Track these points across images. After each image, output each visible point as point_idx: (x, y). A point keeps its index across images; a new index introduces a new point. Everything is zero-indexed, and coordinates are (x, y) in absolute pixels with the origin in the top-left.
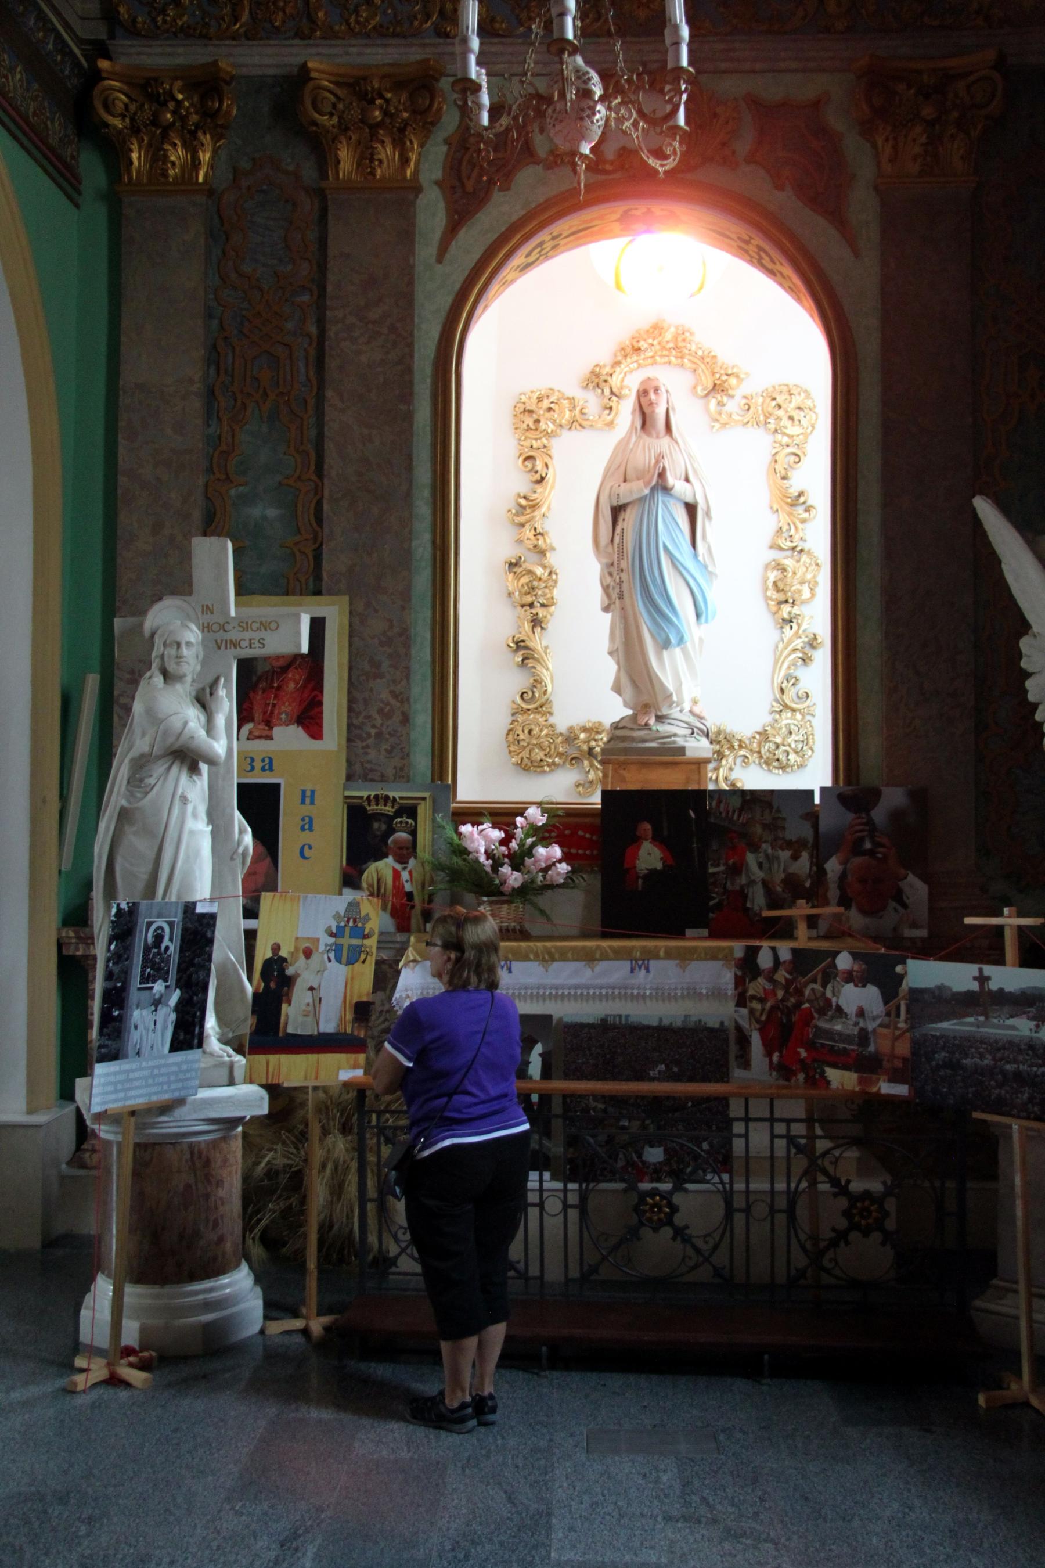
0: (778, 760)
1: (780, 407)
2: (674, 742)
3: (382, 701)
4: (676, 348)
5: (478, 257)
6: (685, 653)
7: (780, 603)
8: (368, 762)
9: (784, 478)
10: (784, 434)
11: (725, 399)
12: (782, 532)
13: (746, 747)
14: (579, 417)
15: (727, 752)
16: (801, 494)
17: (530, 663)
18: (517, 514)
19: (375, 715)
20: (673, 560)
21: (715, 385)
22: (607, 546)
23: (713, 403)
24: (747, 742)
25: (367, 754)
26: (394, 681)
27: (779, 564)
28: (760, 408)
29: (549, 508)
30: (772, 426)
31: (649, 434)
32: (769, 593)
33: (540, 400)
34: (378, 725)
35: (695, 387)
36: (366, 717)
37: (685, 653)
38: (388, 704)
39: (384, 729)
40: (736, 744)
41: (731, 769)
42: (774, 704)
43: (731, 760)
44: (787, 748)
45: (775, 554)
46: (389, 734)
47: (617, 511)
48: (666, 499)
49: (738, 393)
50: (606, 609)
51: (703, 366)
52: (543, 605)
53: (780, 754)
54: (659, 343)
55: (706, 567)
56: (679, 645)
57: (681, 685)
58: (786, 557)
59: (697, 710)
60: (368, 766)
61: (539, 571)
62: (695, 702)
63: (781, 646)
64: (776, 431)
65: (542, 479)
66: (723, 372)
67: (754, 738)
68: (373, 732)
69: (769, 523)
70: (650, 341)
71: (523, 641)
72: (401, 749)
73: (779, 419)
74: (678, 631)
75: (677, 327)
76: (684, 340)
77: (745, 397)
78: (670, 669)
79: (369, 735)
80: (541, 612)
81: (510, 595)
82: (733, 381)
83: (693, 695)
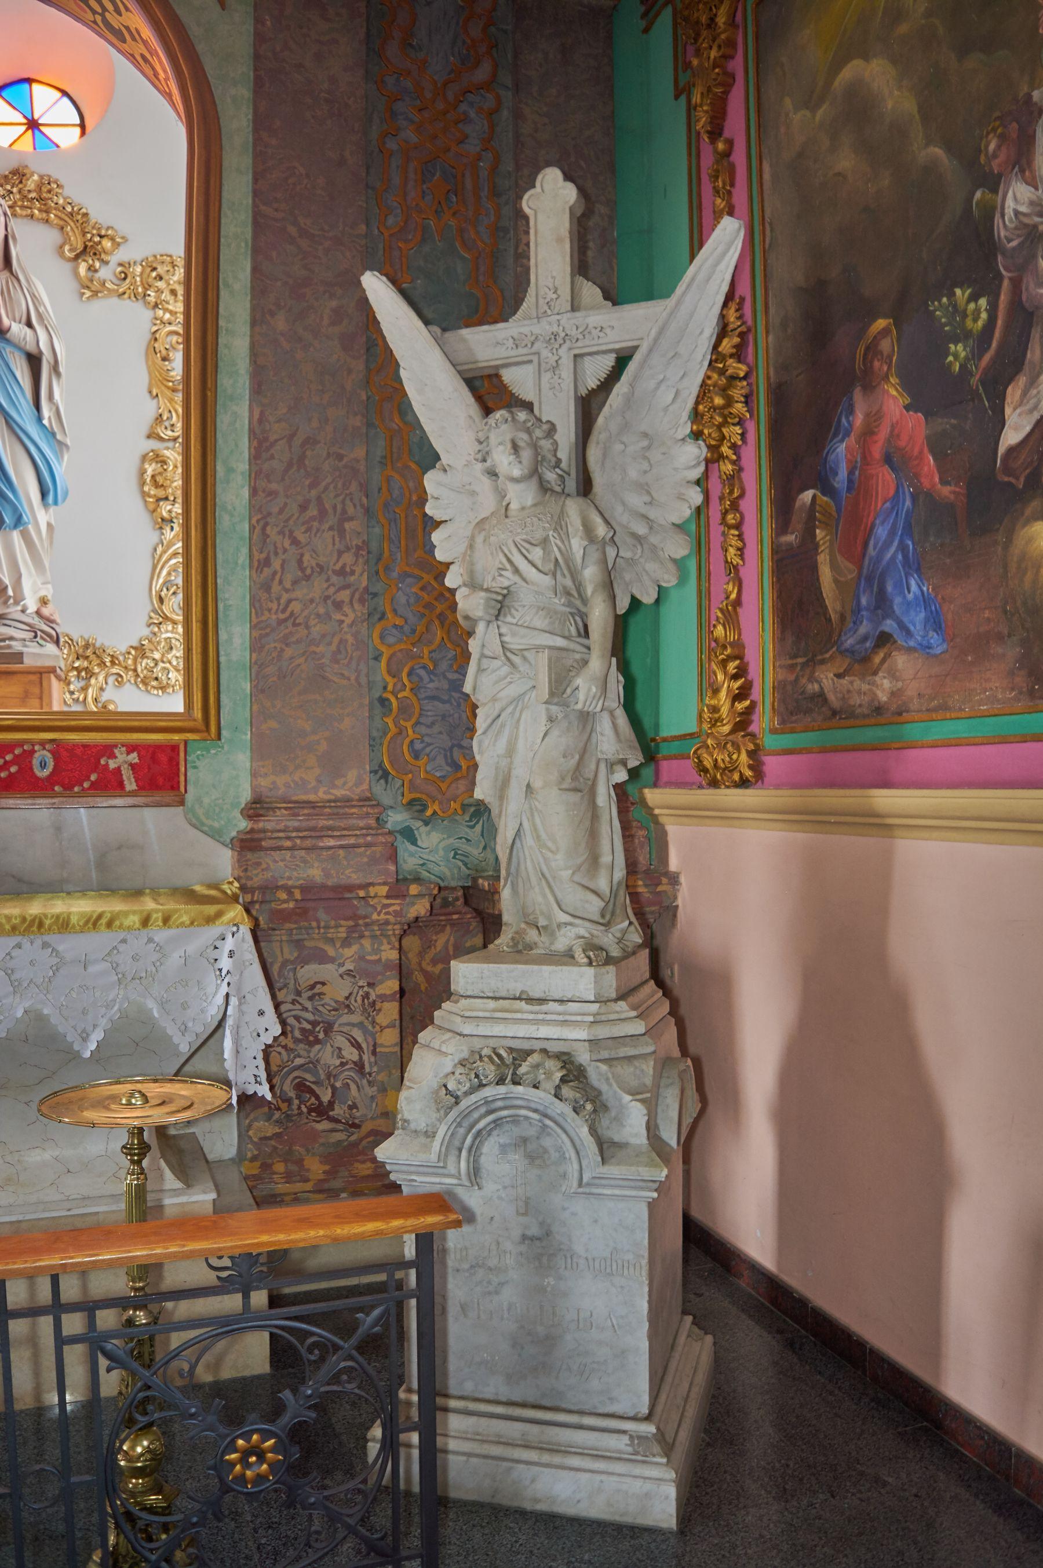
0: (156, 679)
1: (161, 278)
2: (9, 647)
4: (40, 199)
6: (26, 536)
9: (164, 359)
10: (166, 310)
11: (97, 264)
12: (162, 421)
13: (120, 664)
15: (96, 670)
21: (86, 247)
24: (121, 658)
27: (157, 456)
28: (138, 279)
30: (152, 299)
32: (146, 489)
35: (61, 247)
37: (26, 536)
40: (108, 660)
41: (102, 689)
42: (152, 615)
43: (101, 678)
44: (168, 665)
45: (154, 444)
49: (114, 259)
51: (72, 224)
53: (158, 672)
54: (20, 192)
55: (54, 434)
56: (15, 527)
57: (20, 576)
58: (167, 448)
59: (45, 611)
62: (44, 601)
63: (160, 549)
64: (156, 306)
66: (95, 232)
67: (129, 653)
70: (8, 187)
73: (159, 291)
74: (15, 509)
75: (41, 177)
76: (49, 191)
77: (121, 265)
82: (107, 244)
83: (42, 593)
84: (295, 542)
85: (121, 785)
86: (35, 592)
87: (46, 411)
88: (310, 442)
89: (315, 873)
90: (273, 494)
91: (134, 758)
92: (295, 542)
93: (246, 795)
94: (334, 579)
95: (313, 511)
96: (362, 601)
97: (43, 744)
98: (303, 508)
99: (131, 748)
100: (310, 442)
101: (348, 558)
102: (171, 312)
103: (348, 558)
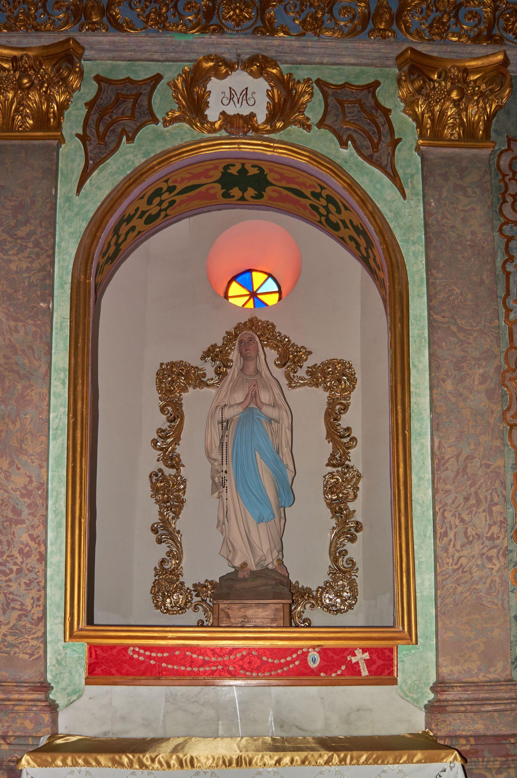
3: (22, 543)
5: (107, 192)
8: (11, 593)
19: (16, 553)
25: (9, 586)
26: (32, 526)
34: (19, 563)
36: (8, 556)
38: (27, 545)
39: (24, 566)
46: (28, 570)
60: (11, 596)
68: (15, 568)
72: (38, 583)
79: (11, 571)
84: (462, 521)
85: (359, 673)
88: (470, 458)
89: (479, 727)
90: (448, 492)
91: (367, 656)
92: (462, 521)
93: (433, 679)
94: (487, 543)
95: (472, 501)
96: (505, 555)
97: (314, 647)
98: (467, 499)
99: (364, 650)
100: (470, 458)
101: (495, 529)
103: (495, 529)
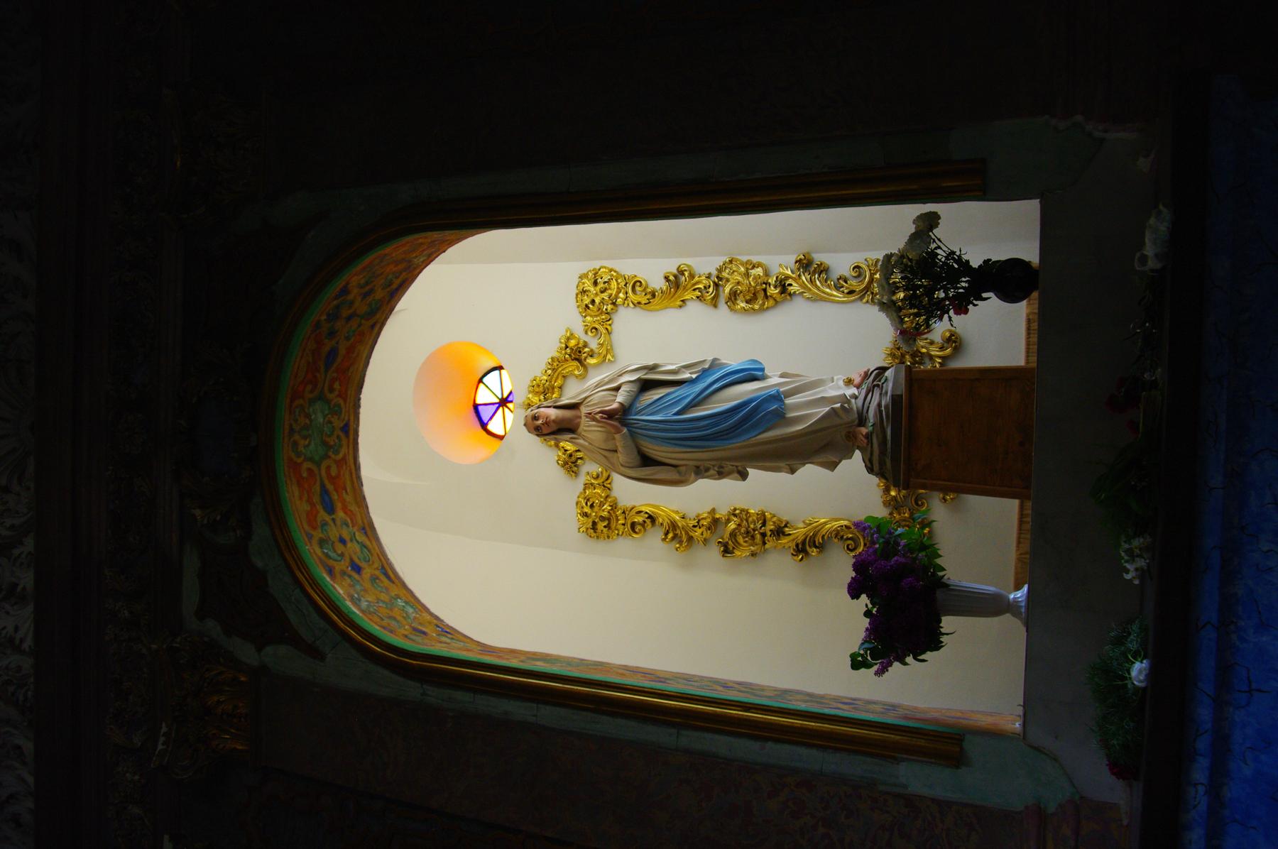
1: (593, 302)
2: (886, 407)
7: (766, 297)
9: (654, 296)
10: (617, 297)
14: (600, 481)
16: (667, 278)
17: (819, 539)
18: (681, 542)
20: (695, 403)
22: (679, 473)
23: (591, 361)
29: (677, 512)
30: (610, 307)
31: (578, 425)
32: (757, 307)
33: (586, 515)
41: (932, 343)
45: (722, 300)
47: (646, 461)
48: (634, 410)
49: (584, 338)
50: (744, 476)
52: (764, 524)
55: (704, 371)
57: (823, 398)
59: (857, 380)
61: (732, 526)
62: (849, 382)
64: (614, 304)
65: (650, 517)
69: (694, 308)
71: (797, 545)
78: (806, 411)
80: (770, 526)
81: (753, 554)
83: (841, 383)
86: (839, 388)
87: (686, 375)
102: (619, 291)
